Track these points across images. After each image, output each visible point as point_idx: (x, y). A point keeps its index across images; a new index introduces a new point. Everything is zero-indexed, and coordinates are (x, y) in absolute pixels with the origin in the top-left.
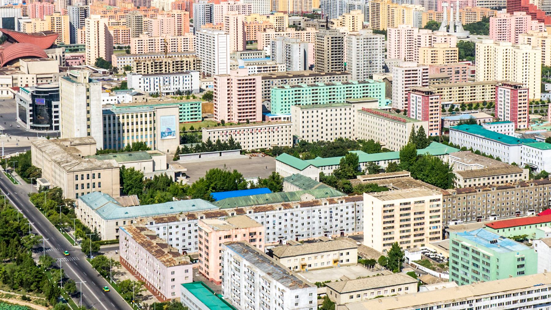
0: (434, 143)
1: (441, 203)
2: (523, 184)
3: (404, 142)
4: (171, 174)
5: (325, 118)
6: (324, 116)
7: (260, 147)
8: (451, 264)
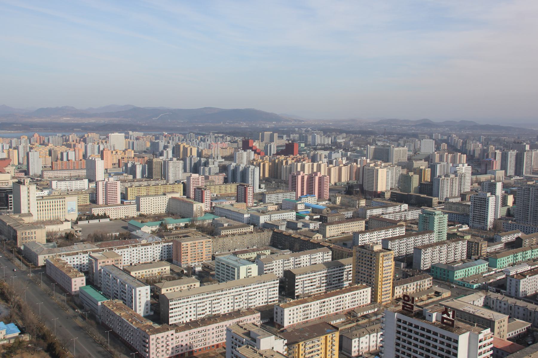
1: (211, 243)
2: (251, 232)
4: (73, 231)
7: (119, 217)
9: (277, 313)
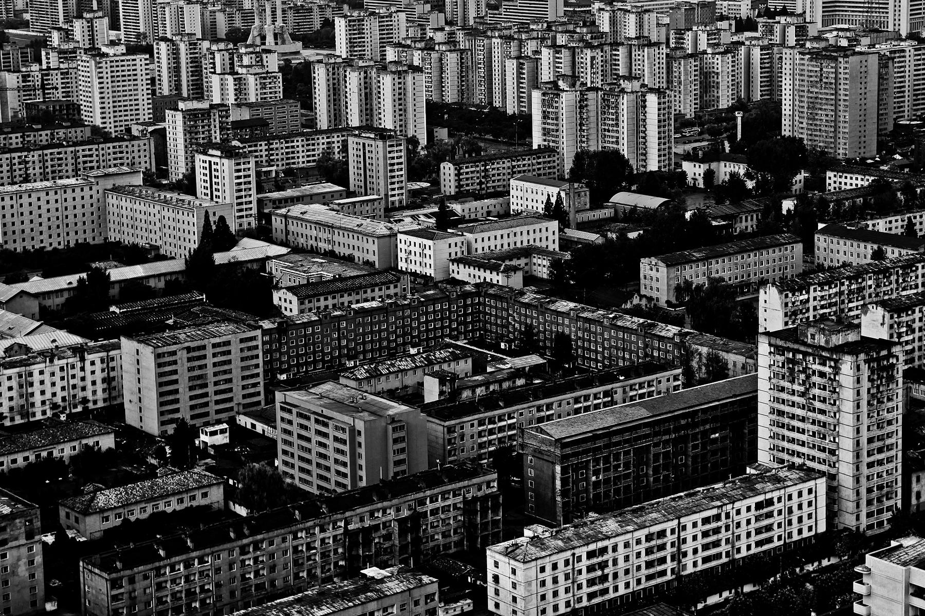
0: (246, 242)
3: (192, 242)
5: (45, 207)
6: (42, 203)
8: (281, 446)
9: (496, 578)
